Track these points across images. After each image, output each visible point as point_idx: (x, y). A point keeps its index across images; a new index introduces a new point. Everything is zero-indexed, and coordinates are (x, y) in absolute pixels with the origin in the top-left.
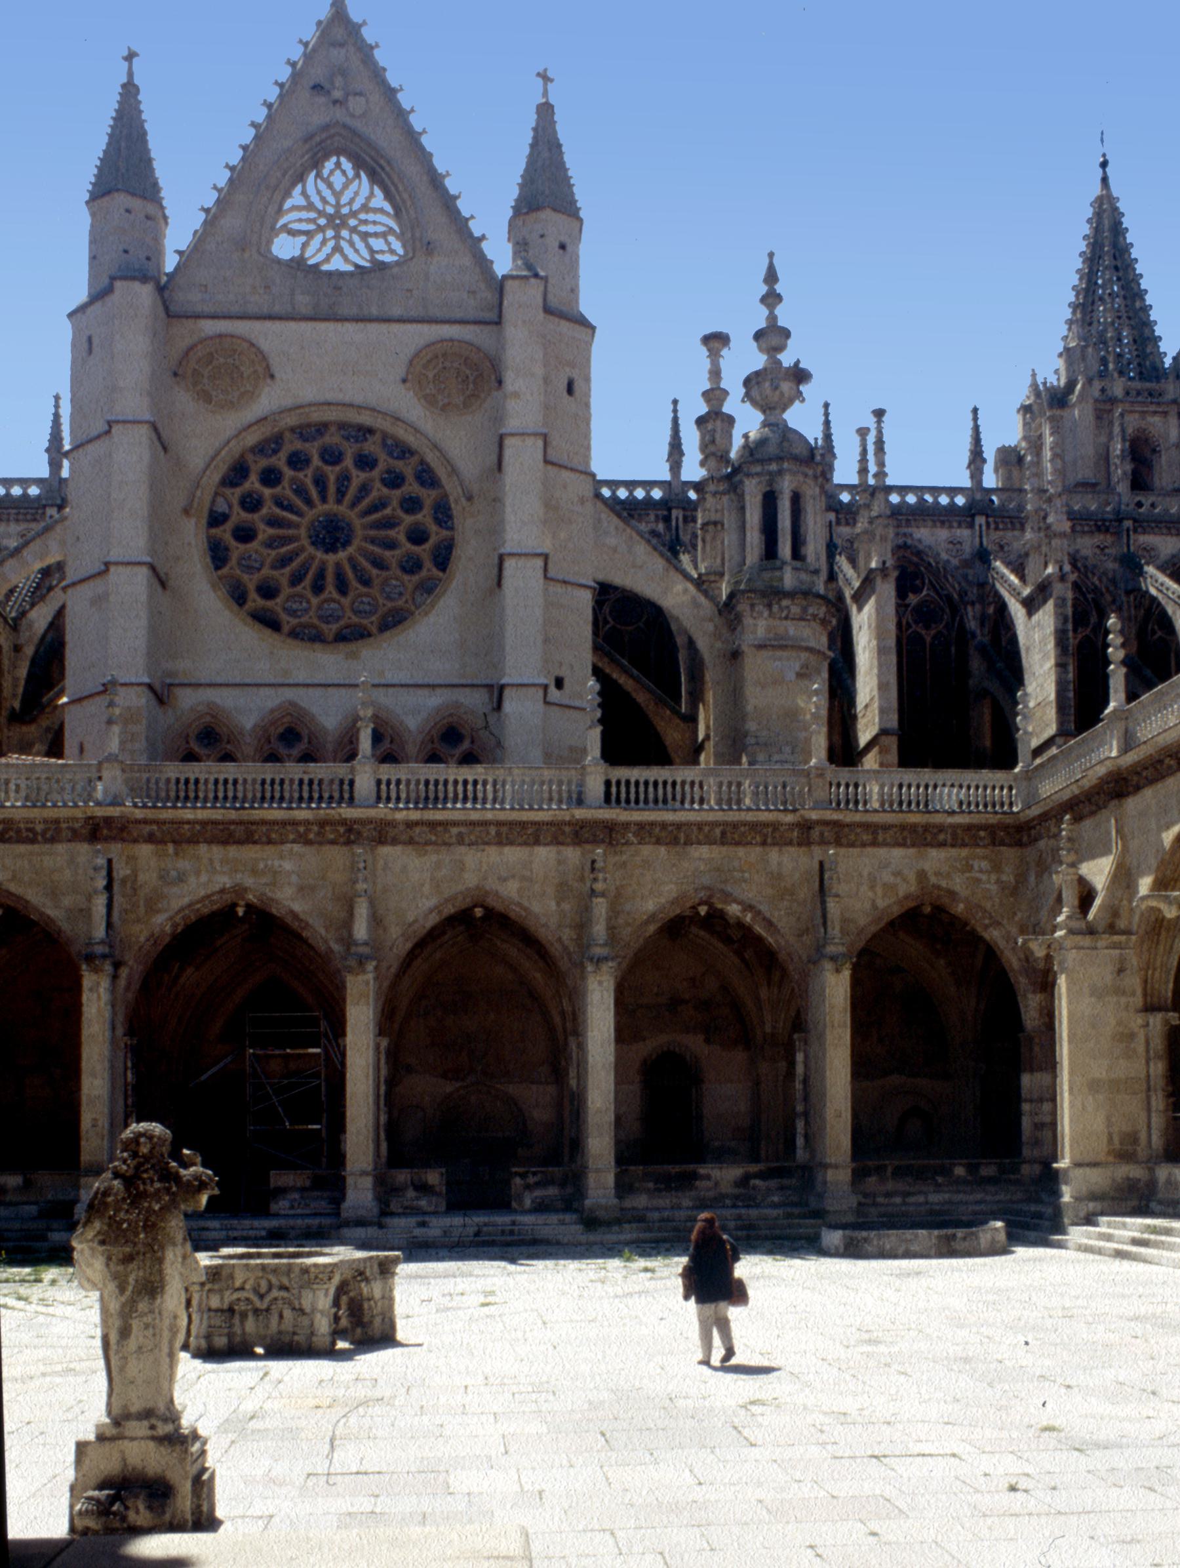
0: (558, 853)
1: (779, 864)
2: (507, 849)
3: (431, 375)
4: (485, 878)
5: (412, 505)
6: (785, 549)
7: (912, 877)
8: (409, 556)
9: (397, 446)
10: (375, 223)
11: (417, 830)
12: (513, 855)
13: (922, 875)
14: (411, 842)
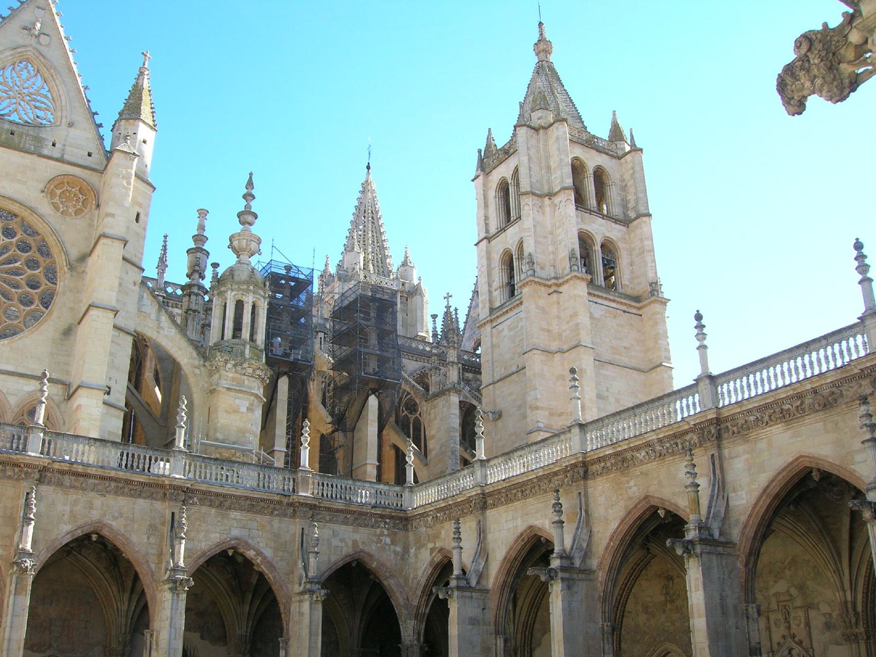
0: (152, 504)
1: (279, 527)
2: (120, 498)
3: (58, 192)
4: (105, 515)
5: (32, 264)
6: (246, 334)
7: (350, 543)
8: (27, 294)
9: (30, 228)
10: (43, 103)
11: (66, 477)
12: (122, 503)
13: (355, 542)
14: (60, 484)
